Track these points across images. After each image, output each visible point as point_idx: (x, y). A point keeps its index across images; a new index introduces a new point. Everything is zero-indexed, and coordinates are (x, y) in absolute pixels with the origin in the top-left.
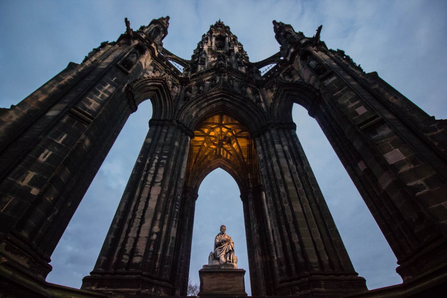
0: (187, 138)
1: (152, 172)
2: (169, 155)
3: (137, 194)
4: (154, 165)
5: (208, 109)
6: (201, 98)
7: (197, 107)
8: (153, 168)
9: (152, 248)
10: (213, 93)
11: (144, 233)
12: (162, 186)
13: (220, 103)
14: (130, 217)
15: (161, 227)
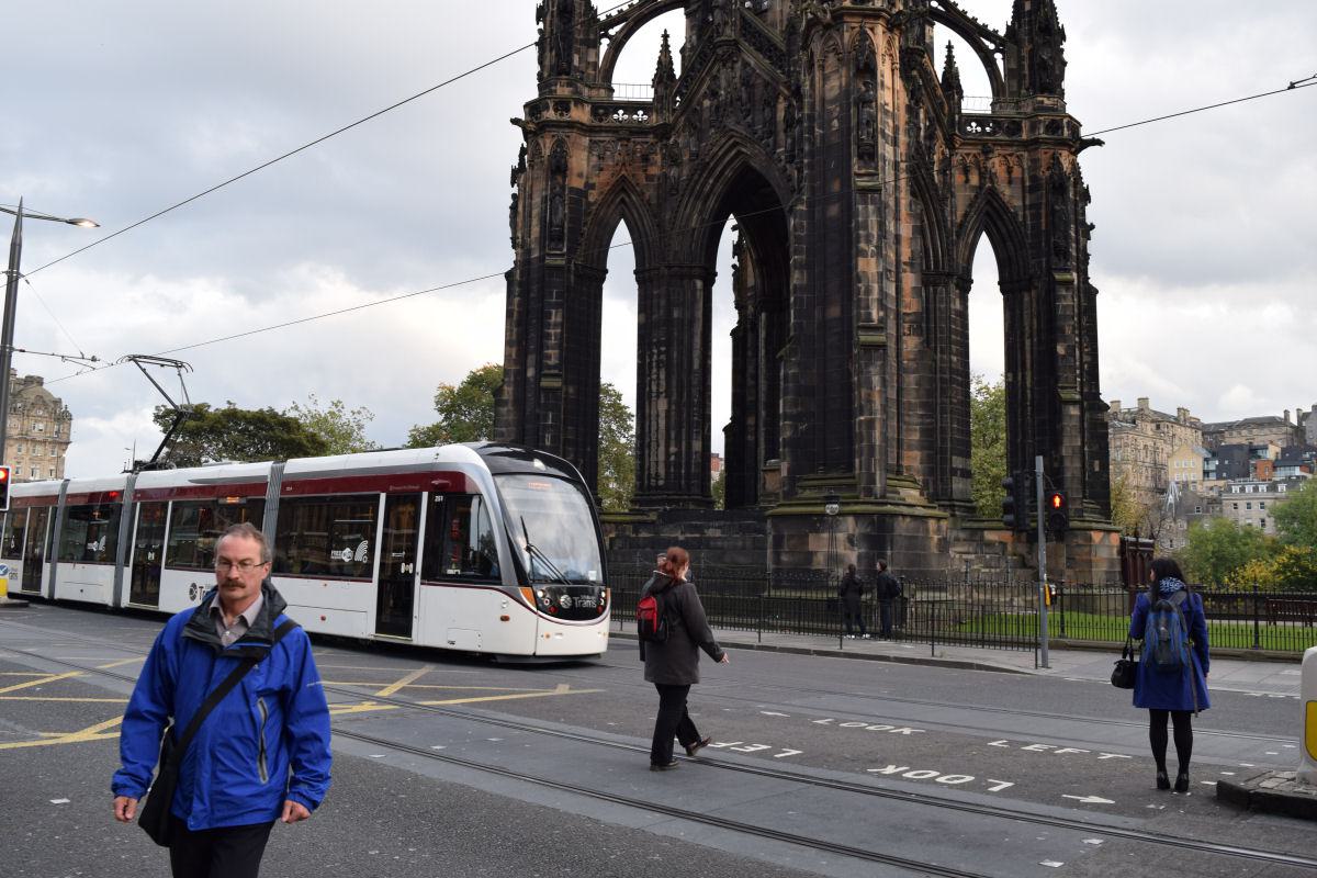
0: (695, 284)
1: (654, 377)
2: (668, 344)
3: (647, 411)
4: (654, 364)
5: (719, 188)
6: (696, 177)
7: (697, 198)
8: (654, 370)
9: (672, 470)
10: (715, 149)
11: (662, 457)
12: (668, 396)
13: (737, 163)
14: (647, 441)
15: (678, 444)
